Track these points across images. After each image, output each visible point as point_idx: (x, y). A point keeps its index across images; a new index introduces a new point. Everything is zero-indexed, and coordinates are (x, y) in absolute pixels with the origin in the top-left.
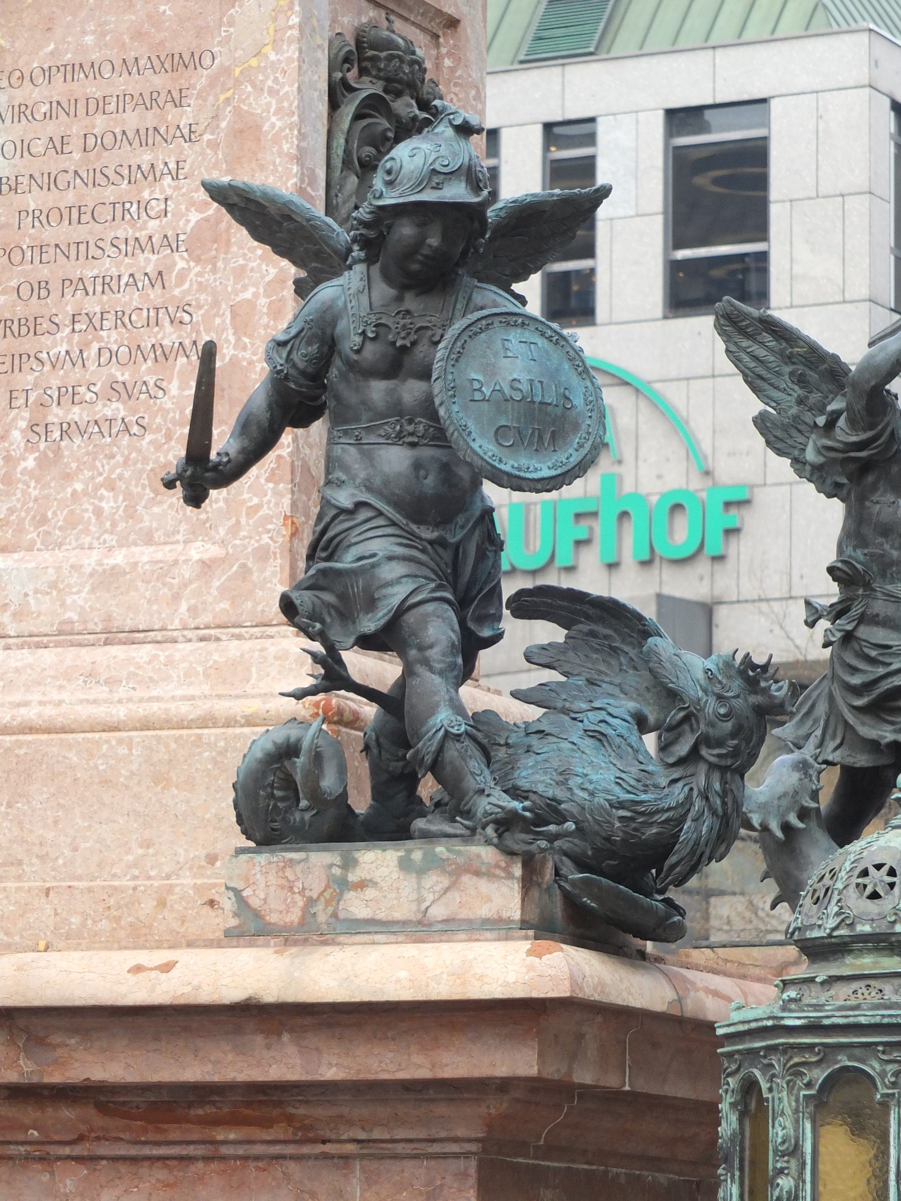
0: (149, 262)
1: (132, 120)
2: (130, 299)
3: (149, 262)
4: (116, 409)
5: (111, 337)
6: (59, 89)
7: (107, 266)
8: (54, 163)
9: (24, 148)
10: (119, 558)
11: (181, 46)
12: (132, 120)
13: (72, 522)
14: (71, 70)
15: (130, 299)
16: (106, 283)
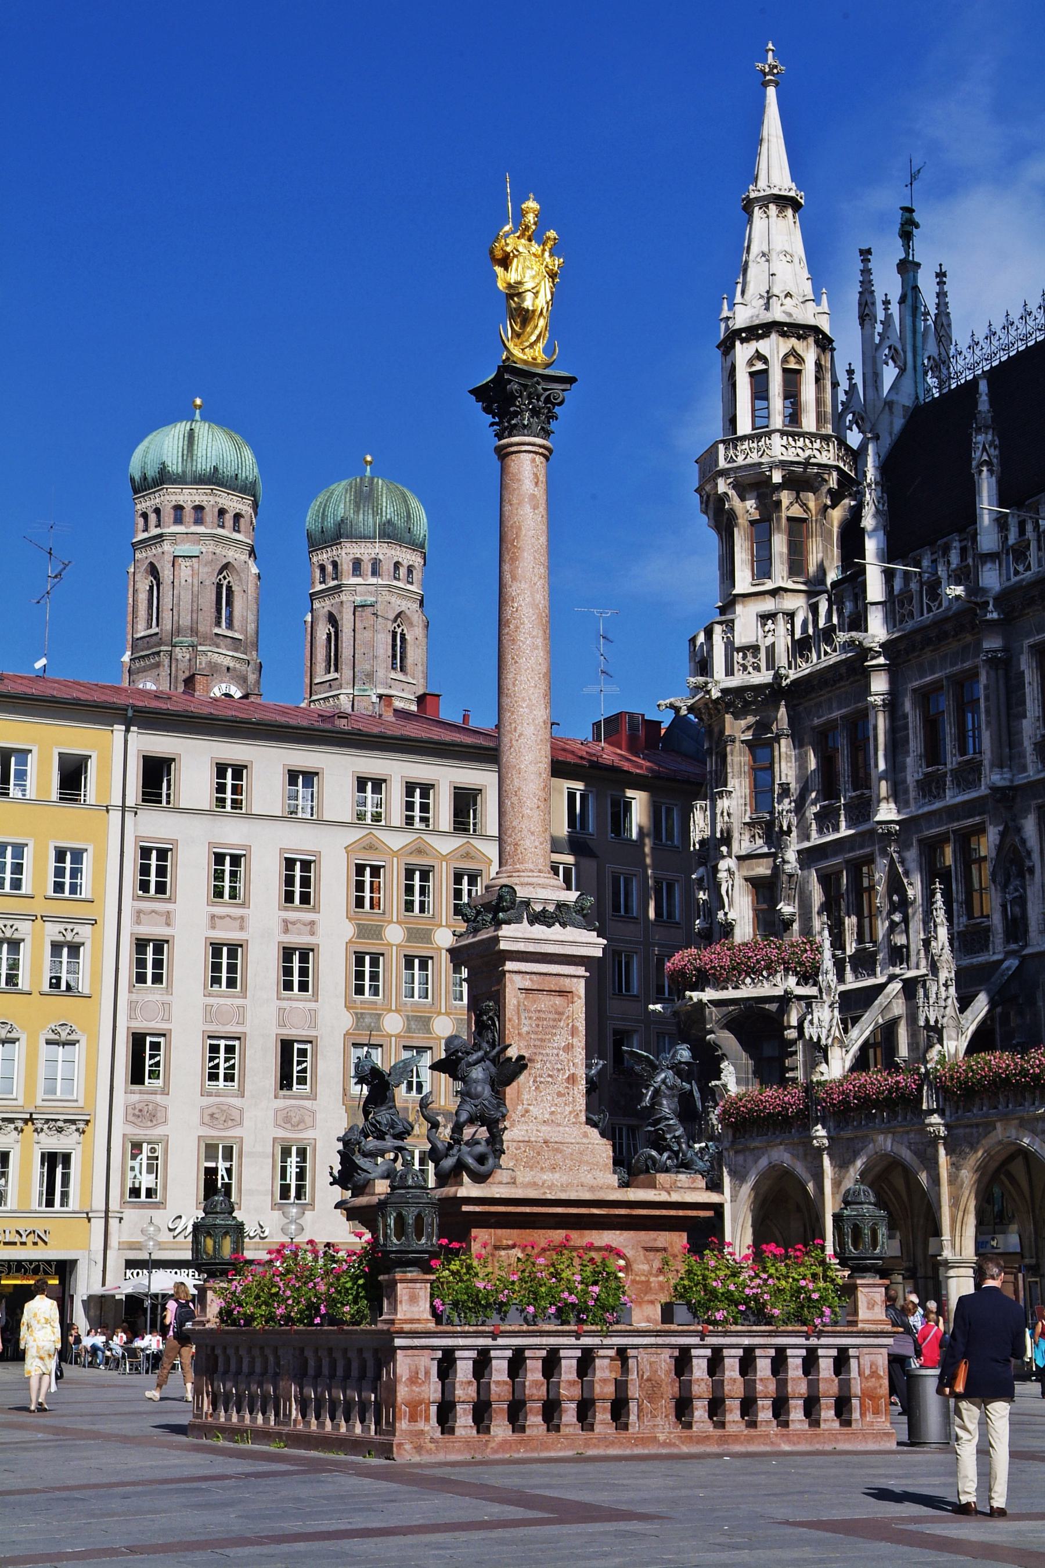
0: (555, 1052)
1: (551, 1023)
2: (551, 1058)
3: (555, 1052)
4: (550, 1079)
5: (548, 1065)
6: (537, 1015)
7: (548, 1051)
8: (537, 1029)
9: (531, 1025)
10: (553, 1109)
11: (561, 1010)
12: (551, 1023)
13: (542, 1101)
14: (539, 1011)
15: (551, 1058)
16: (548, 1055)
